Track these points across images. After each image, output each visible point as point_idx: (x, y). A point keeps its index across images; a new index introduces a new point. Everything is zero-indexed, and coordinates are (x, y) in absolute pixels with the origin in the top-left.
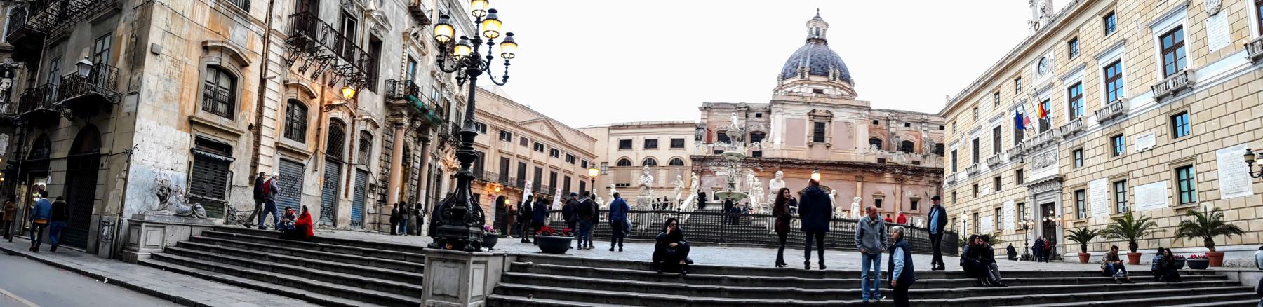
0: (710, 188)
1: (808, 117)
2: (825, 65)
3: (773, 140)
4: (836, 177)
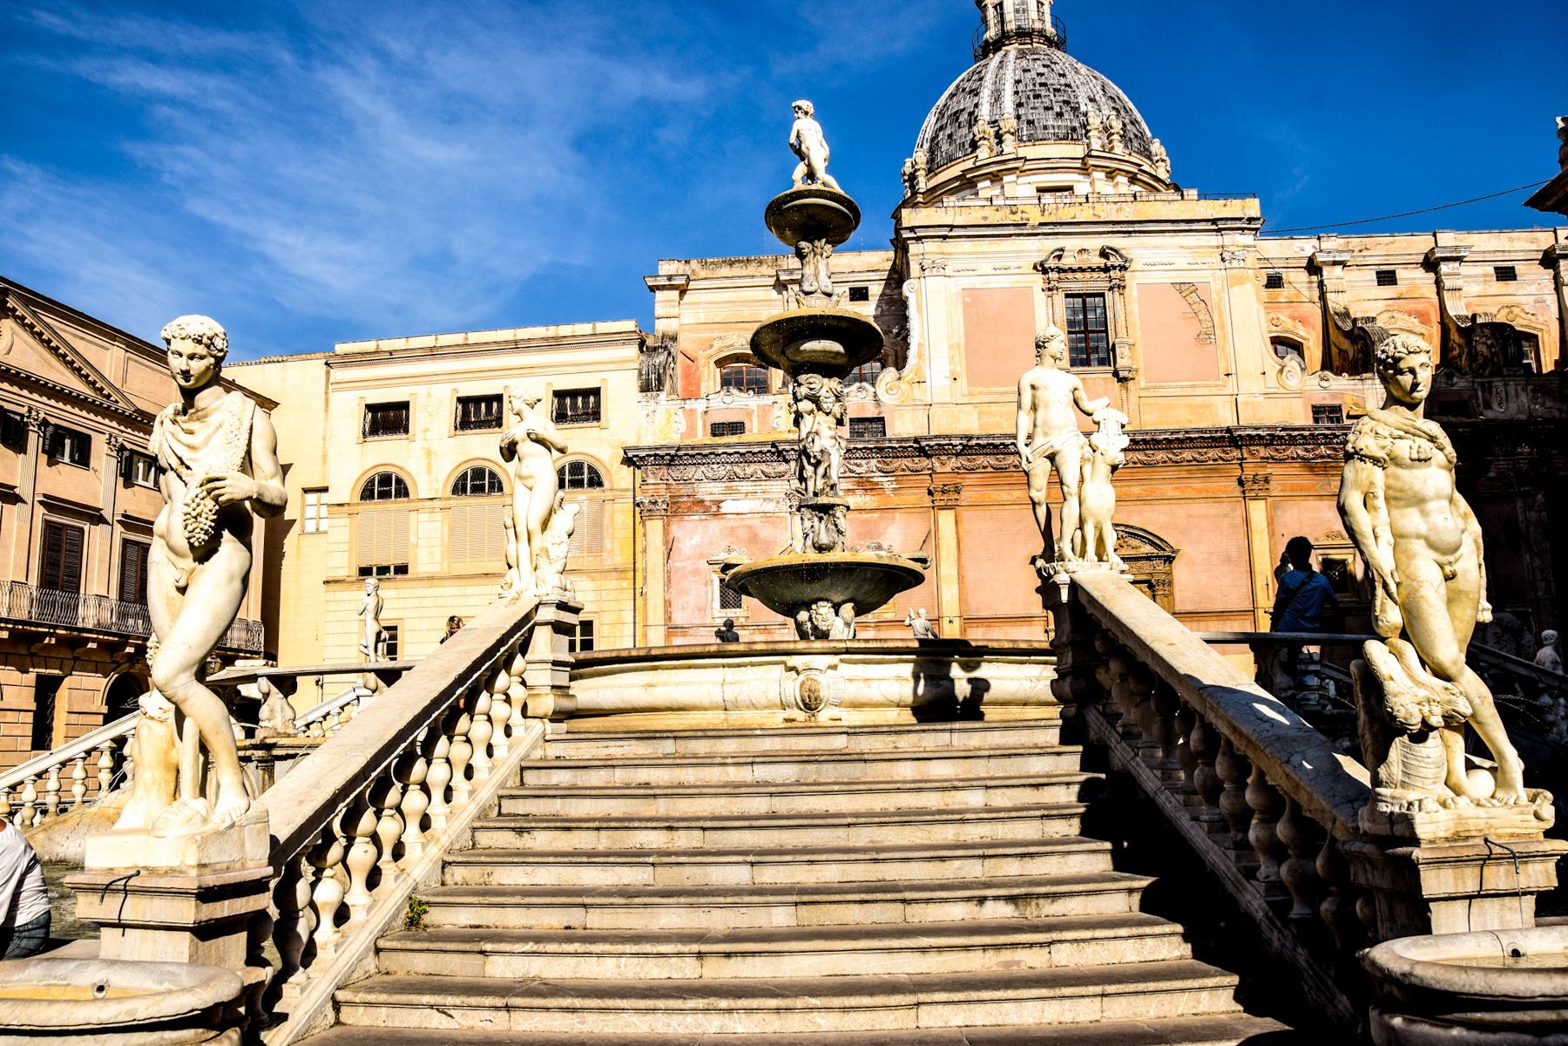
0: (703, 565)
1: (1039, 277)
2: (1067, 102)
3: (918, 370)
4: (1169, 490)
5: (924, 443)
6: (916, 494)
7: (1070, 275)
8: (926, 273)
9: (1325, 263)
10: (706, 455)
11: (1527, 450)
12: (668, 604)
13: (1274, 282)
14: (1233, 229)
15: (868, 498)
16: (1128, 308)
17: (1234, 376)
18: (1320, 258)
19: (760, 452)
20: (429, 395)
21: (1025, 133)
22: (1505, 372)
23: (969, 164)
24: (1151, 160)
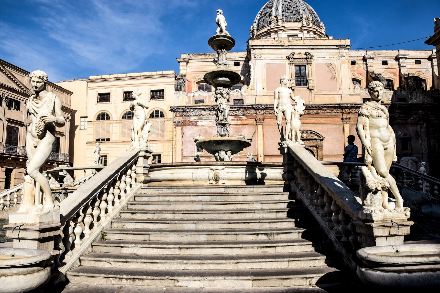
1: (288, 60)
2: (297, 11)
3: (253, 86)
4: (322, 121)
5: (254, 107)
6: (252, 121)
7: (296, 60)
8: (256, 59)
9: (368, 58)
10: (193, 109)
11: (422, 112)
12: (182, 150)
13: (353, 63)
14: (342, 48)
15: (238, 121)
16: (312, 70)
17: (341, 89)
18: (367, 57)
19: (208, 108)
20: (116, 91)
21: (285, 19)
22: (417, 90)
23: (269, 28)
24: (320, 28)
